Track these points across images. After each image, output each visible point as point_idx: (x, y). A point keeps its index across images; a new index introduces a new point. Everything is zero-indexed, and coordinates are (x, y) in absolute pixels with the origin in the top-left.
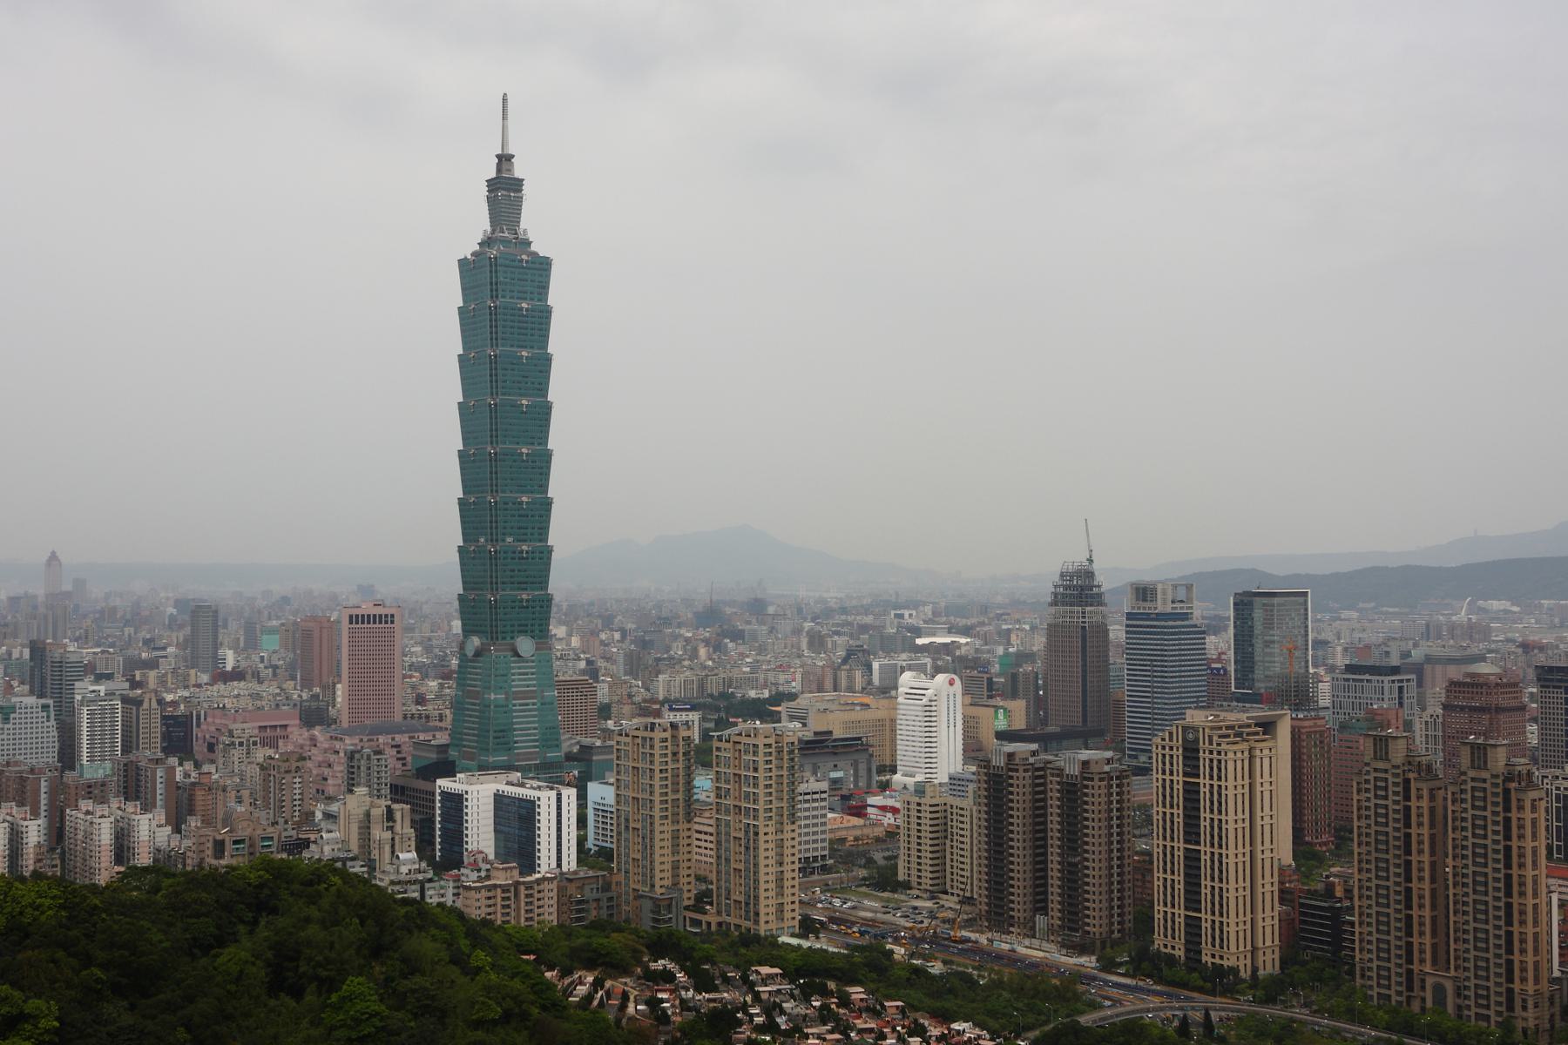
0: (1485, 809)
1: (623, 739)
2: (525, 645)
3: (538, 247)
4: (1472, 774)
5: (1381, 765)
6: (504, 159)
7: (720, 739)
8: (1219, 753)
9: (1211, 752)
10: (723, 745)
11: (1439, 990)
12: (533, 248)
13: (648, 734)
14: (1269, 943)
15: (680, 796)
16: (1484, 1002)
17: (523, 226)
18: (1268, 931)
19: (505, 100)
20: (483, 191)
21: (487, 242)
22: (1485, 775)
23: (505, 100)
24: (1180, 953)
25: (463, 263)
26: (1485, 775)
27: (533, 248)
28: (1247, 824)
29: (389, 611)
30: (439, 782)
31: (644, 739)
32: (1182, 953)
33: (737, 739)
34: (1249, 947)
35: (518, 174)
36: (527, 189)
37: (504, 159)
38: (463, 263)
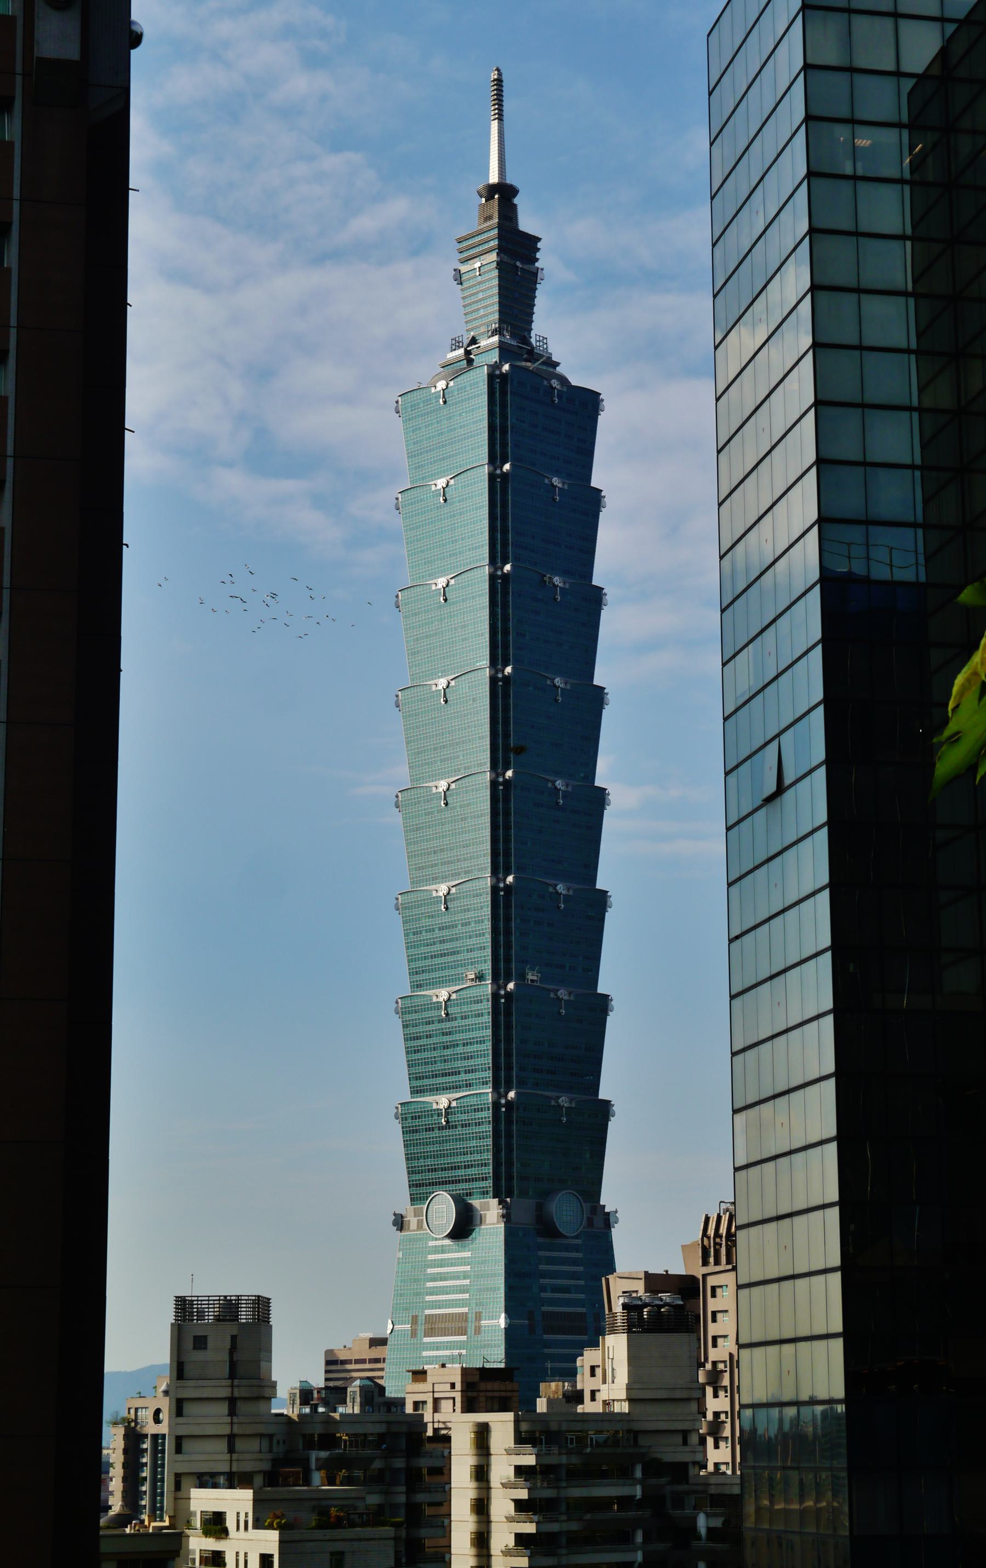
19: (499, 82)
23: (499, 82)
35: (527, 223)
36: (544, 260)
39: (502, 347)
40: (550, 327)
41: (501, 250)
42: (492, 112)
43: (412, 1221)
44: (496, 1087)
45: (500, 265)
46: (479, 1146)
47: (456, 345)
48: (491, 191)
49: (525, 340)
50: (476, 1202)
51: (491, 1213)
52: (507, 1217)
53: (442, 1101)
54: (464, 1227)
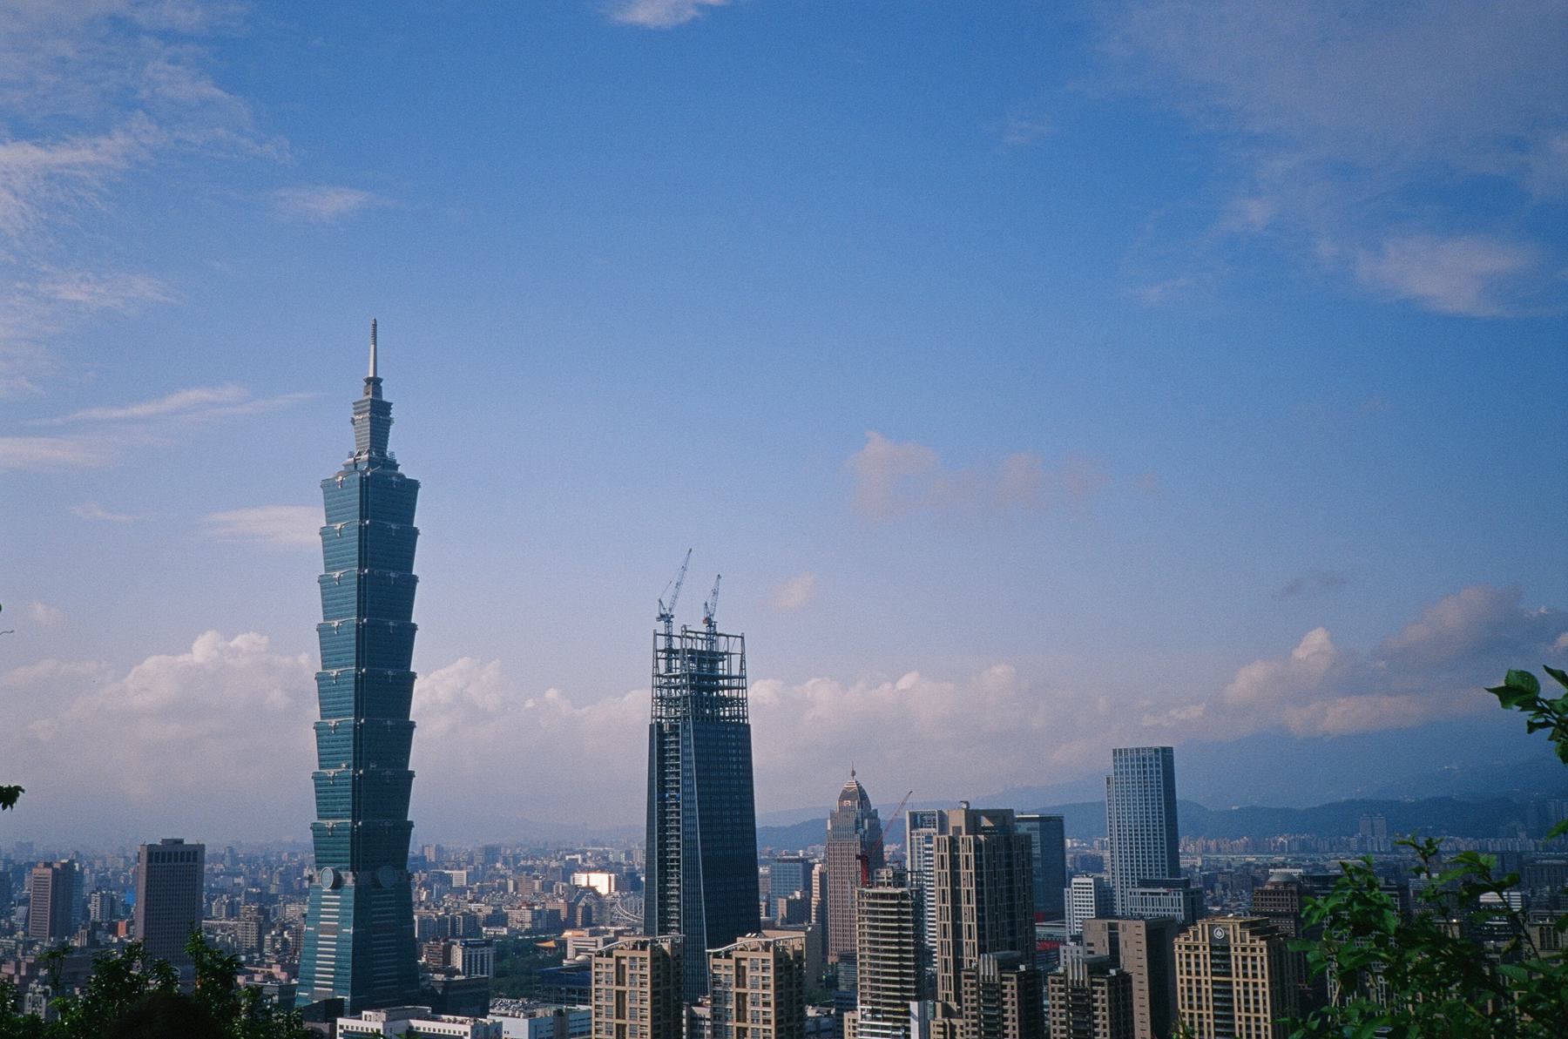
1: (604, 960)
2: (386, 875)
3: (407, 470)
6: (375, 383)
7: (717, 956)
9: (1244, 950)
10: (723, 962)
12: (400, 470)
13: (638, 954)
19: (375, 326)
20: (351, 413)
23: (375, 326)
25: (328, 486)
27: (400, 470)
30: (340, 1021)
31: (633, 959)
33: (741, 955)
35: (384, 398)
36: (393, 414)
38: (328, 486)
39: (371, 462)
40: (393, 447)
41: (372, 411)
42: (370, 340)
43: (317, 879)
44: (353, 818)
45: (371, 419)
46: (345, 848)
47: (351, 455)
48: (368, 380)
49: (383, 454)
50: (343, 873)
51: (349, 880)
52: (356, 881)
53: (330, 823)
54: (337, 884)
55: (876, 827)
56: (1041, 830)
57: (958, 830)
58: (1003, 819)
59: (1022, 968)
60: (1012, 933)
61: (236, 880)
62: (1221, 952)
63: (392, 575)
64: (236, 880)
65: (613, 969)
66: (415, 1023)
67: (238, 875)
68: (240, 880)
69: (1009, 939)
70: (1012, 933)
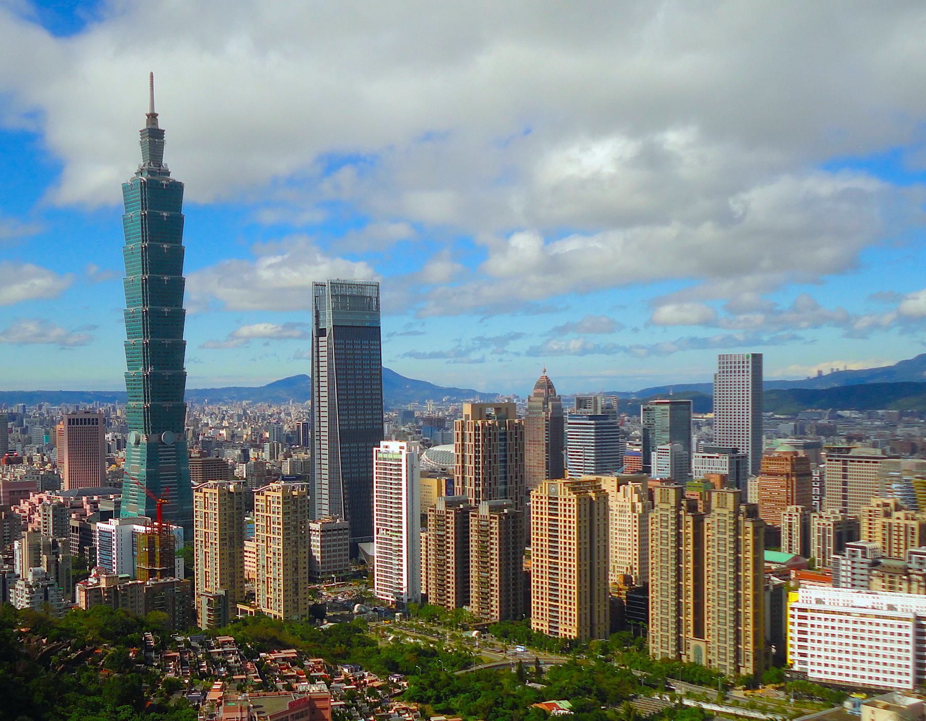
0: (725, 533)
4: (718, 511)
5: (665, 506)
8: (570, 500)
9: (565, 500)
11: (698, 650)
12: (172, 176)
14: (602, 621)
15: (235, 531)
16: (723, 657)
17: (165, 161)
18: (602, 614)
21: (141, 172)
22: (726, 512)
24: (546, 629)
26: (726, 512)
27: (172, 176)
28: (588, 546)
29: (95, 417)
32: (547, 628)
34: (588, 623)
35: (160, 127)
37: (153, 117)
40: (169, 160)
55: (558, 409)
56: (671, 409)
57: (467, 416)
58: (505, 410)
59: (461, 506)
60: (506, 483)
61: (221, 432)
62: (553, 501)
63: (165, 246)
64: (221, 432)
65: (202, 500)
66: (136, 527)
67: (223, 428)
68: (223, 432)
69: (503, 487)
70: (506, 483)
